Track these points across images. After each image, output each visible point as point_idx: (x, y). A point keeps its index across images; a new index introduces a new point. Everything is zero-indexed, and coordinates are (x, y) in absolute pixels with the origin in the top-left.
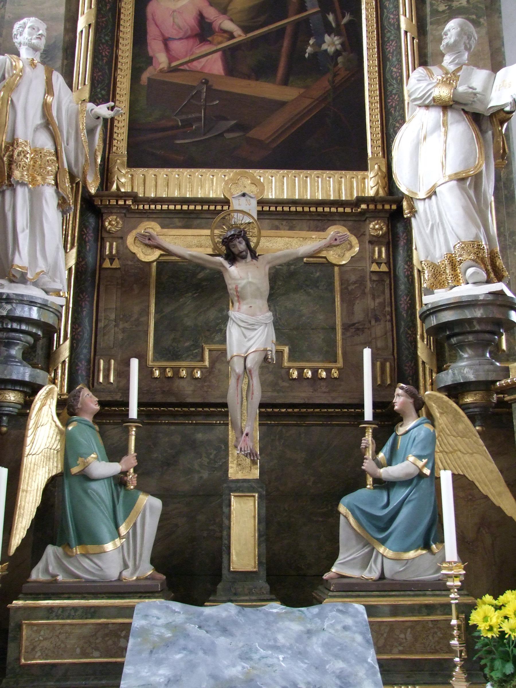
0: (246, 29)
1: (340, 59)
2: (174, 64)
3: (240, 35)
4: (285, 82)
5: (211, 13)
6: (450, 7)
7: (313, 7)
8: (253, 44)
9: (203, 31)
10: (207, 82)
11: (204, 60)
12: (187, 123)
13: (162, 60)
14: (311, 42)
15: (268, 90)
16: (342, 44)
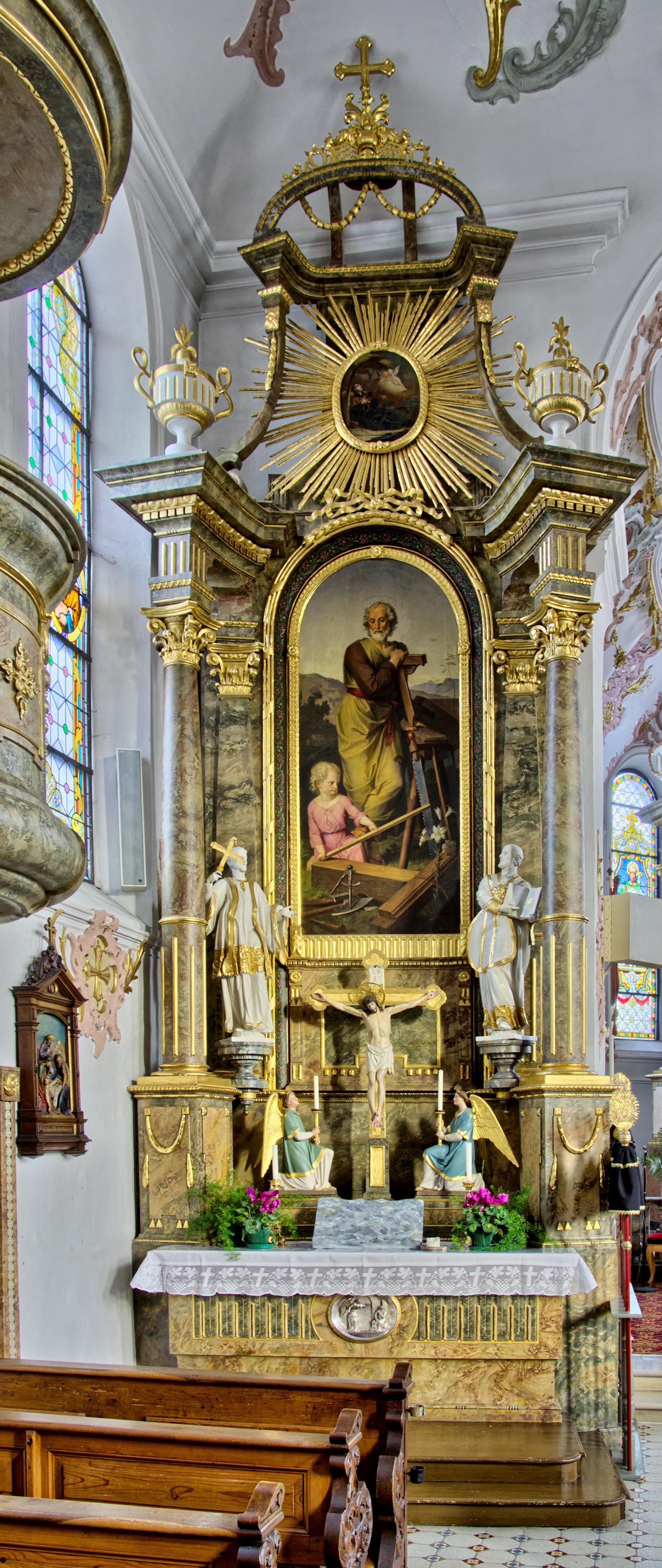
0: (378, 824)
1: (444, 846)
2: (329, 854)
3: (374, 830)
4: (405, 867)
5: (353, 811)
6: (517, 814)
7: (425, 802)
8: (383, 836)
9: (348, 826)
10: (351, 868)
11: (349, 850)
12: (340, 900)
13: (320, 850)
14: (424, 832)
15: (394, 873)
16: (446, 834)
